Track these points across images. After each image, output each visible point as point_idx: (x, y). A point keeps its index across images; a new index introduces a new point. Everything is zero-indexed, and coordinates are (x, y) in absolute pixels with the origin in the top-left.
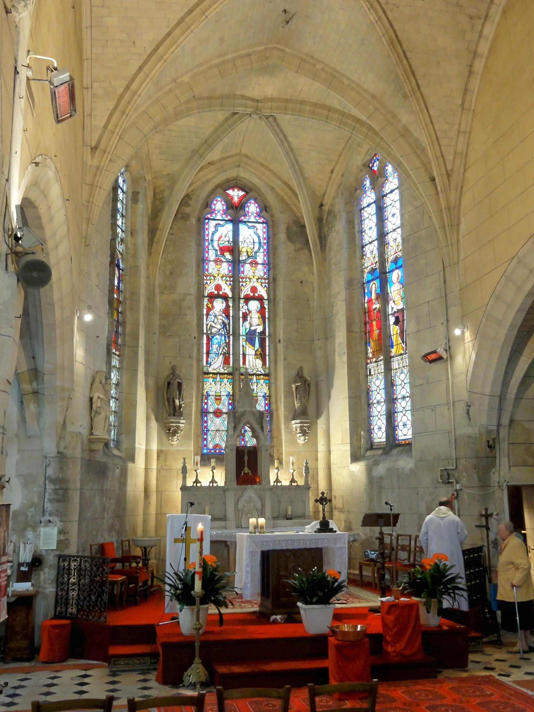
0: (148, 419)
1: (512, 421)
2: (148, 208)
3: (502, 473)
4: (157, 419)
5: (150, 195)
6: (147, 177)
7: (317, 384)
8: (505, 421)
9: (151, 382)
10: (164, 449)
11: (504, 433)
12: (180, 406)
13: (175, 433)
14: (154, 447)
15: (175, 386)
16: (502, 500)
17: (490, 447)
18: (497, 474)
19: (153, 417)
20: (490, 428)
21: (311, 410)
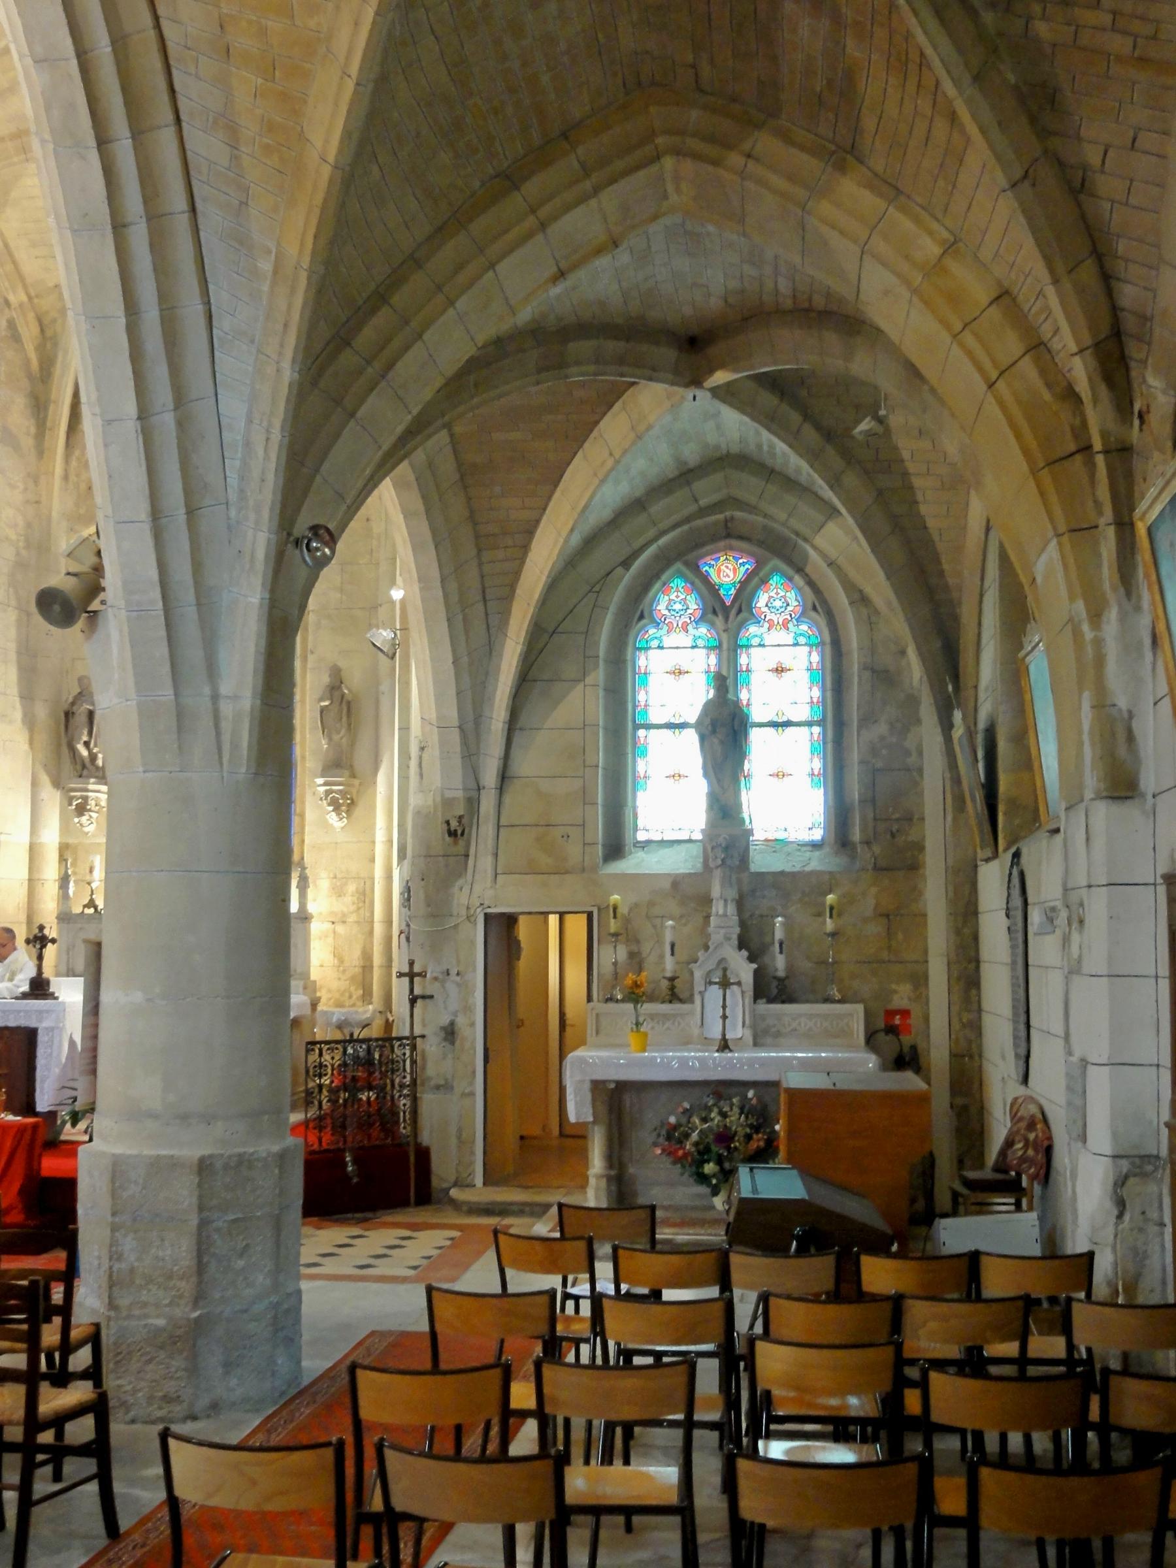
0: (35, 784)
1: (504, 777)
2: (27, 362)
3: (477, 888)
4: (57, 784)
5: (29, 332)
6: (12, 298)
7: (377, 702)
8: (490, 778)
9: (42, 712)
10: (70, 841)
11: (488, 804)
12: (93, 757)
13: (81, 810)
14: (51, 837)
15: (81, 718)
16: (473, 943)
17: (452, 834)
18: (466, 890)
19: (45, 779)
20: (449, 794)
21: (361, 756)
